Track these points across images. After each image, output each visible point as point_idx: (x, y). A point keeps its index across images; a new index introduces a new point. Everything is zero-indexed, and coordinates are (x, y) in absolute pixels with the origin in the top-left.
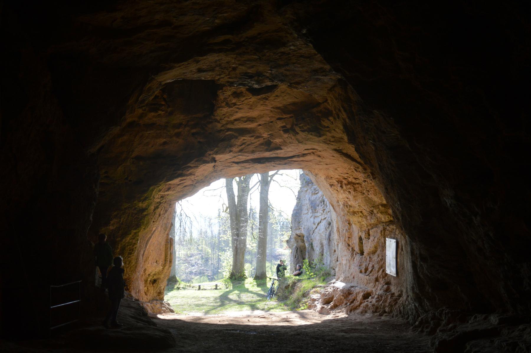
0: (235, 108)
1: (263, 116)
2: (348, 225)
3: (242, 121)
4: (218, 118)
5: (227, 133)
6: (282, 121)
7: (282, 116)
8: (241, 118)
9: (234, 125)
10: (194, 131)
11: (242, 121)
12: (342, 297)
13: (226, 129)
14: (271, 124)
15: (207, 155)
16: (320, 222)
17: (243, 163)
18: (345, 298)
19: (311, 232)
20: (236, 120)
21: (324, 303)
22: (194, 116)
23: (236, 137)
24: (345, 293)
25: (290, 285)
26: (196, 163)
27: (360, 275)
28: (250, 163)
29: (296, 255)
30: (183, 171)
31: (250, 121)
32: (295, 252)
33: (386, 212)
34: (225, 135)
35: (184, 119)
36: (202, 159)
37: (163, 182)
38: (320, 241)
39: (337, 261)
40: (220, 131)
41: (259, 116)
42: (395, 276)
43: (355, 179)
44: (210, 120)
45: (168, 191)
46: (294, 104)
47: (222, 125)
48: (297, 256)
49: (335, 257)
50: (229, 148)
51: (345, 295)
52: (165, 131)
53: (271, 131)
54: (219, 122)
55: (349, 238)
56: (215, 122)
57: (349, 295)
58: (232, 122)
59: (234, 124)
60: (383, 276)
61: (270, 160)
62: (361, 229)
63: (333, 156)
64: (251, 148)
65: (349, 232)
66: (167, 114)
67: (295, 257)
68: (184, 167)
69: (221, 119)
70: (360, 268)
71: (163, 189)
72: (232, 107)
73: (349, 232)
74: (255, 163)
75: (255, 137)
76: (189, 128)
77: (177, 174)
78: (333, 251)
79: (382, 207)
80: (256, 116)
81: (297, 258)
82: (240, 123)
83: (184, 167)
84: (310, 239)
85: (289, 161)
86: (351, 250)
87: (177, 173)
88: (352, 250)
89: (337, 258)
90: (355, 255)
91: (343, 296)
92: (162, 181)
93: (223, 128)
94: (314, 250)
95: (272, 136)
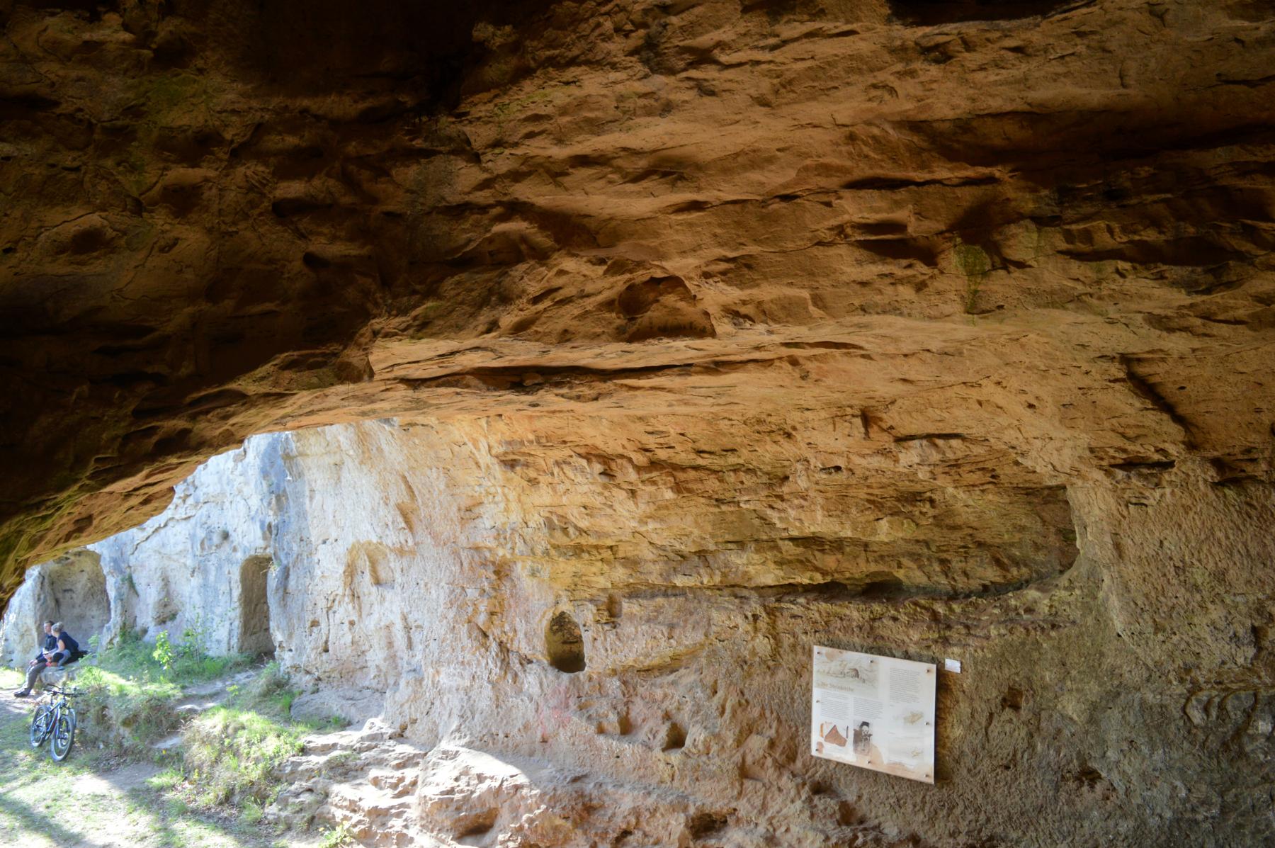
0: (689, 79)
1: (771, 160)
2: (494, 577)
3: (618, 170)
4: (480, 135)
5: (499, 228)
6: (902, 194)
7: (923, 166)
8: (622, 154)
9: (558, 185)
10: (294, 189)
11: (618, 170)
12: (559, 822)
13: (499, 203)
14: (777, 206)
15: (362, 335)
16: (166, 525)
17: (438, 386)
18: (576, 825)
19: (129, 550)
20: (583, 161)
21: (457, 834)
22: (306, 102)
23: (542, 256)
24: (573, 808)
25: (143, 715)
26: (288, 375)
27: (601, 740)
28: (468, 386)
29: (39, 595)
30: (193, 418)
31: (665, 175)
32: (39, 588)
33: (801, 562)
34: (488, 235)
35: (234, 112)
36: (335, 355)
37: (76, 488)
38: (159, 574)
39: (326, 651)
40: (460, 210)
41: (737, 154)
42: (931, 781)
43: (699, 452)
44: (418, 143)
45: (77, 538)
46: (1033, 116)
47: (486, 176)
48: (42, 597)
49: (316, 640)
50: (493, 308)
51: (573, 815)
52: (109, 163)
53: (757, 241)
54: (476, 158)
55: (492, 614)
56: (453, 152)
57: (589, 813)
58: (555, 173)
59: (566, 180)
60: (775, 761)
61: (557, 379)
62: (573, 595)
63: (905, 380)
64: (566, 317)
65: (495, 597)
66: (147, 53)
67: (39, 599)
68: (196, 395)
69: (498, 144)
70: (589, 718)
71: (57, 527)
72: (671, 72)
73: (495, 597)
74: (498, 387)
75: (609, 262)
76: (261, 168)
77: (155, 439)
78: (308, 624)
79: (798, 546)
80: (709, 158)
81: (42, 601)
82: (601, 183)
83: (196, 395)
84: (123, 566)
85: (616, 385)
86: (494, 647)
87: (155, 429)
88: (501, 651)
89: (326, 642)
90: (517, 667)
91: (566, 818)
92: (76, 481)
93: (482, 197)
94: (137, 594)
95: (749, 267)
